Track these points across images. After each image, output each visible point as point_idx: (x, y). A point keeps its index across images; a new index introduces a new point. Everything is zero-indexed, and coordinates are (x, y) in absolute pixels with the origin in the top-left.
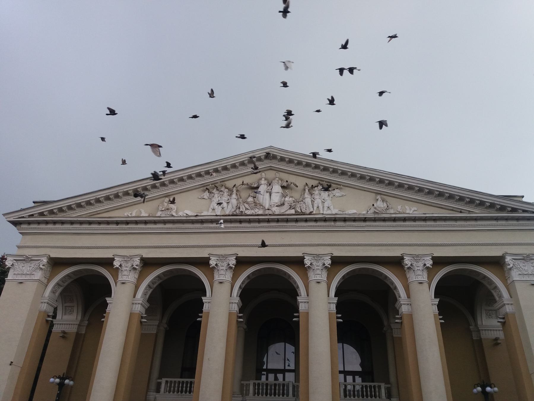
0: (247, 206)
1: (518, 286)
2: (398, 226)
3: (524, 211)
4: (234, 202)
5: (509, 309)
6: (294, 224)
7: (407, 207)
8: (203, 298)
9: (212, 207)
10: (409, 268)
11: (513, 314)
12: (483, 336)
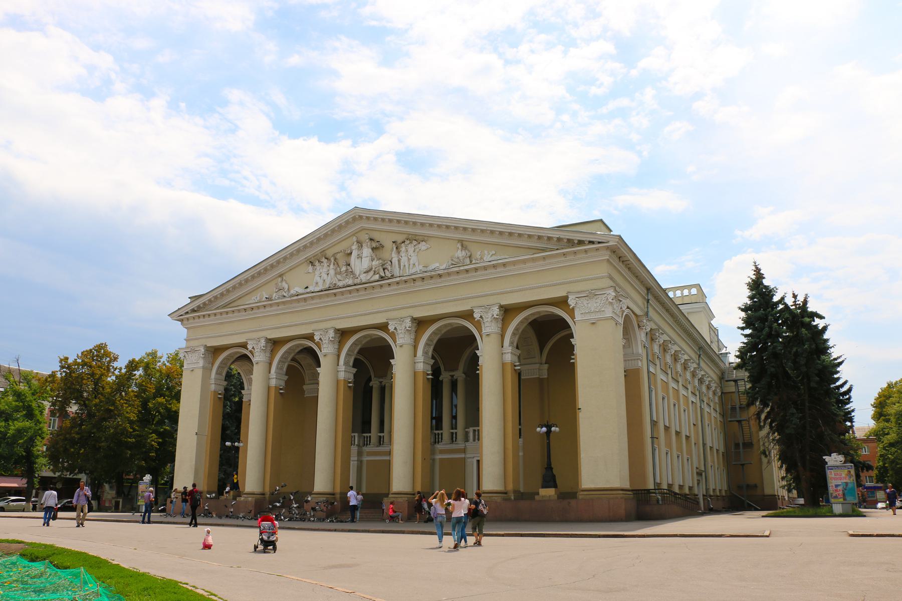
4: (332, 272)
7: (486, 252)
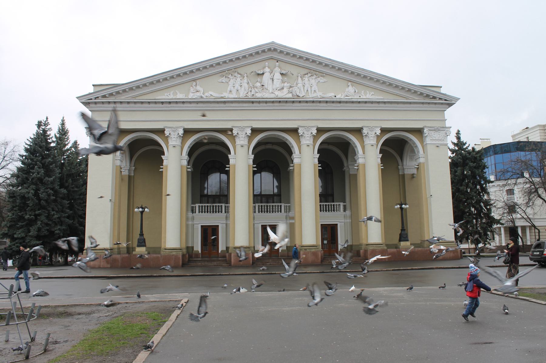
0: (257, 90)
1: (428, 146)
2: (361, 107)
3: (440, 99)
5: (422, 160)
6: (291, 104)
8: (229, 155)
9: (229, 89)
10: (366, 135)
11: (424, 163)
12: (405, 173)
